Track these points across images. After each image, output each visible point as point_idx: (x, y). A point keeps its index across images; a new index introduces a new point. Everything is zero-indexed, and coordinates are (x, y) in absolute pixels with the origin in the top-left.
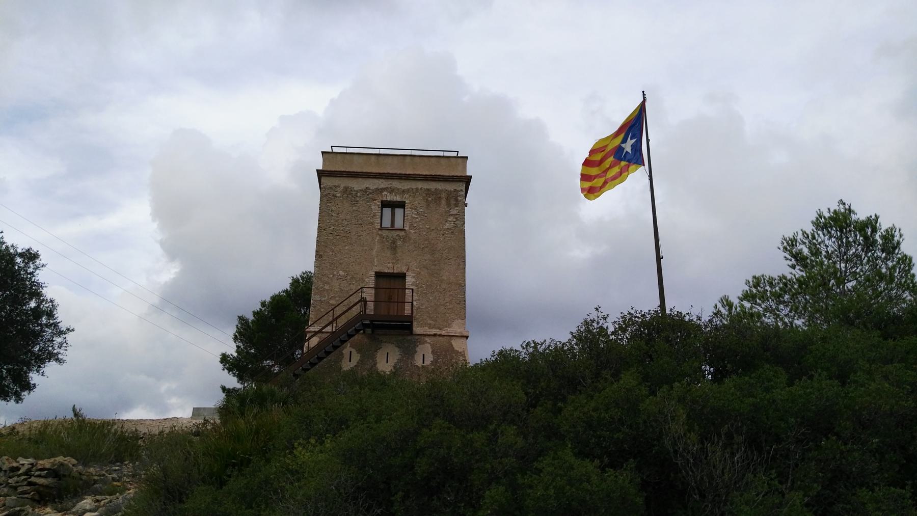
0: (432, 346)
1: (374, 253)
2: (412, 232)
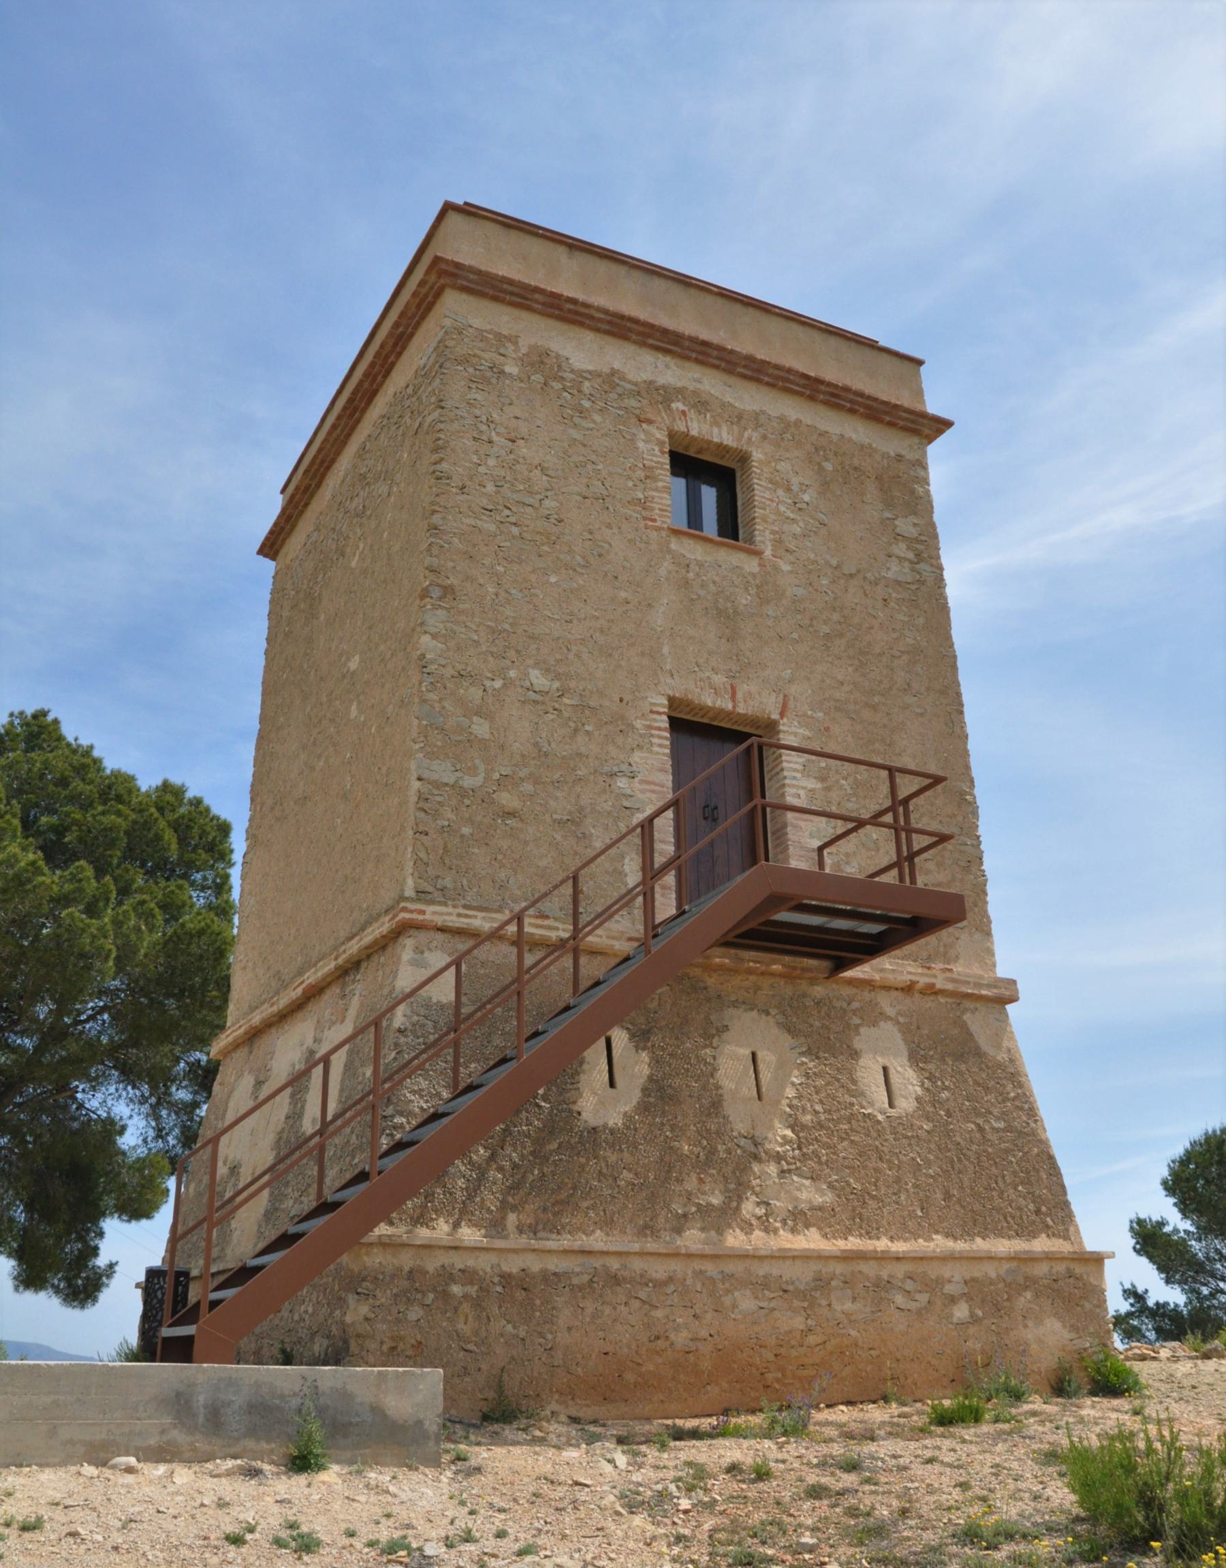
0: (906, 1031)
1: (659, 619)
2: (786, 568)
